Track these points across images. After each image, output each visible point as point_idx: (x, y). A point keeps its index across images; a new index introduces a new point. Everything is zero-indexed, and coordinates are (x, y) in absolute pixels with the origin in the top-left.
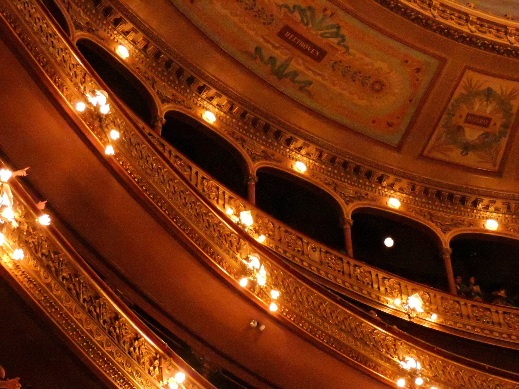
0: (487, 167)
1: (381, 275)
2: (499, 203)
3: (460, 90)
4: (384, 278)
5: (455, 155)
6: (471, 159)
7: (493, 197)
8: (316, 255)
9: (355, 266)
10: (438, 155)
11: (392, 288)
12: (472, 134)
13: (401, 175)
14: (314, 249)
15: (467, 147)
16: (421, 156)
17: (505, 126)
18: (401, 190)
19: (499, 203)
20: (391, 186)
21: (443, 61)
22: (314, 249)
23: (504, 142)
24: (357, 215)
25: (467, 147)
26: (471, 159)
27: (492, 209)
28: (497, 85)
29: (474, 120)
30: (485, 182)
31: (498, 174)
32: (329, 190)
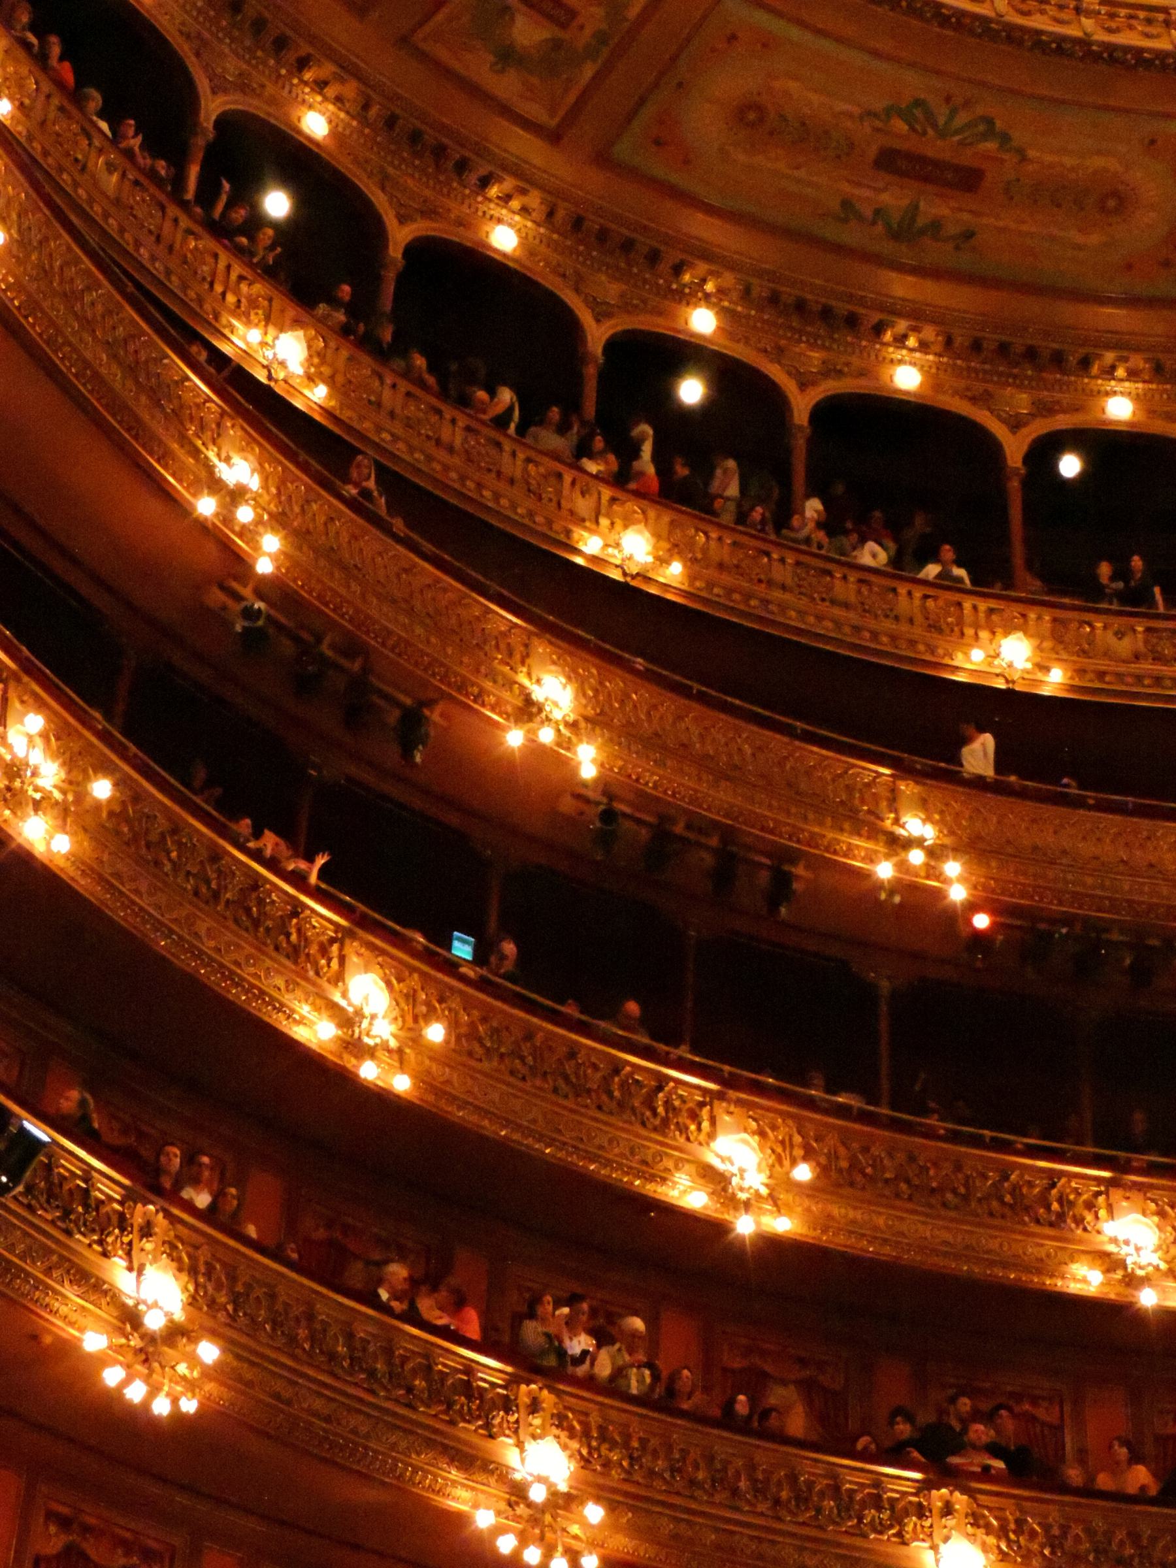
0: (535, 111)
1: (237, 270)
2: (534, 199)
4: (241, 278)
5: (478, 65)
6: (507, 85)
7: (526, 180)
9: (189, 232)
10: (442, 53)
11: (253, 303)
13: (348, 70)
14: (110, 167)
15: (507, 56)
17: (602, 38)
18: (339, 100)
19: (534, 199)
20: (320, 86)
22: (110, 167)
23: (588, 71)
25: (507, 56)
26: (507, 85)
27: (515, 204)
31: (554, 137)
32: (185, 49)
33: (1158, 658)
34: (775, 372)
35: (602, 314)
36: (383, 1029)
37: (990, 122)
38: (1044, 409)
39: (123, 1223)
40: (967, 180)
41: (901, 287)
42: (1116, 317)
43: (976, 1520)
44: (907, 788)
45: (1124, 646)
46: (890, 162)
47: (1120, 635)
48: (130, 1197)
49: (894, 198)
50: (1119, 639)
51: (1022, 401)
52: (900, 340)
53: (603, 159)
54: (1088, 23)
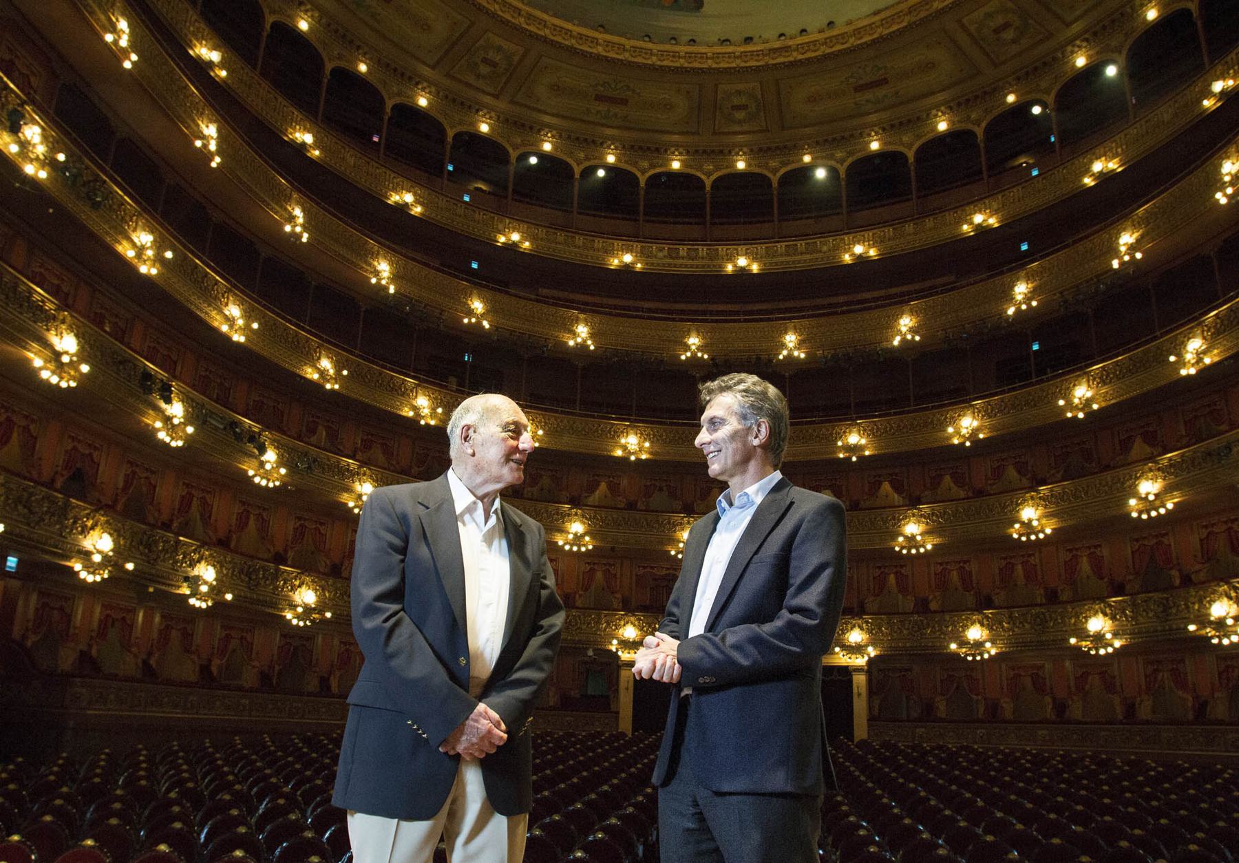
3: (481, 42)
5: (471, 79)
6: (480, 84)
7: (490, 109)
8: (352, 161)
10: (459, 76)
11: (398, 184)
12: (484, 69)
13: (431, 83)
15: (478, 76)
16: (448, 75)
18: (430, 93)
20: (423, 89)
21: (473, 24)
24: (396, 107)
26: (480, 84)
28: (506, 45)
29: (485, 61)
30: (487, 99)
31: (496, 97)
33: (671, 258)
34: (569, 160)
35: (515, 148)
36: (426, 411)
37: (628, 87)
38: (652, 166)
39: (358, 474)
40: (624, 102)
41: (609, 132)
42: (676, 138)
43: (583, 516)
44: (582, 316)
45: (660, 255)
46: (599, 98)
47: (661, 250)
48: (360, 467)
49: (602, 107)
50: (661, 253)
51: (646, 164)
52: (609, 147)
53: (512, 102)
54: (654, 58)
